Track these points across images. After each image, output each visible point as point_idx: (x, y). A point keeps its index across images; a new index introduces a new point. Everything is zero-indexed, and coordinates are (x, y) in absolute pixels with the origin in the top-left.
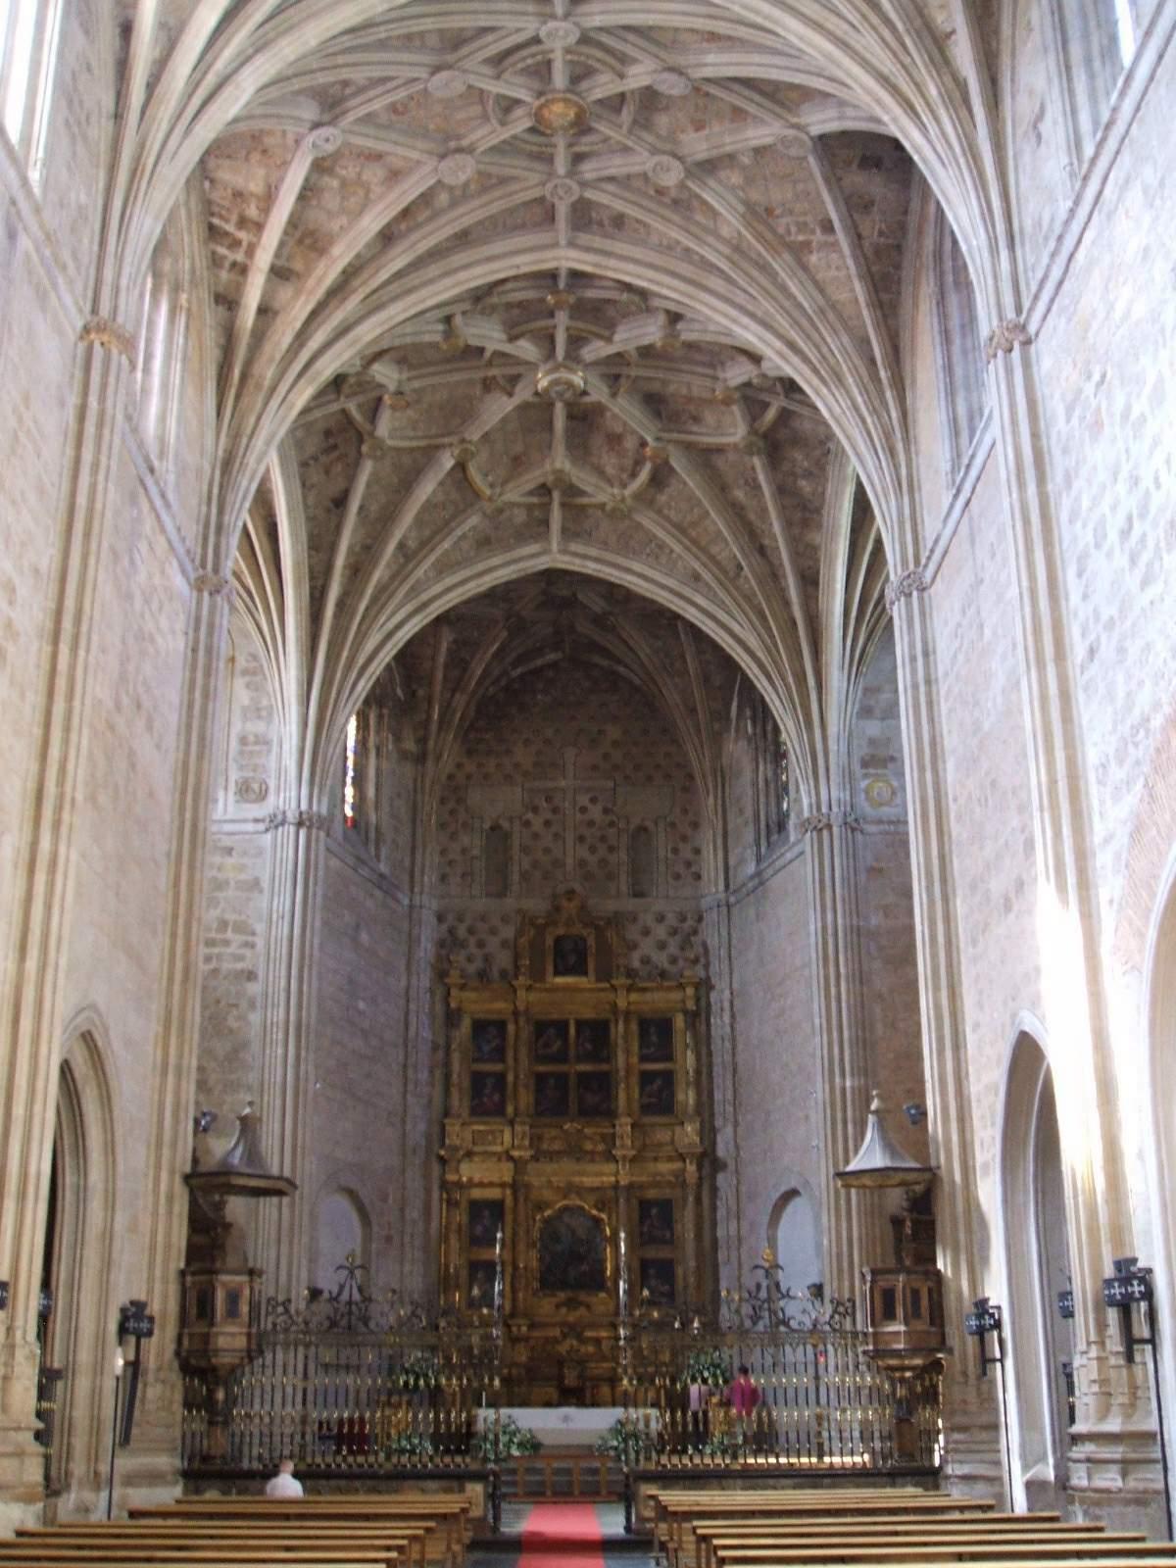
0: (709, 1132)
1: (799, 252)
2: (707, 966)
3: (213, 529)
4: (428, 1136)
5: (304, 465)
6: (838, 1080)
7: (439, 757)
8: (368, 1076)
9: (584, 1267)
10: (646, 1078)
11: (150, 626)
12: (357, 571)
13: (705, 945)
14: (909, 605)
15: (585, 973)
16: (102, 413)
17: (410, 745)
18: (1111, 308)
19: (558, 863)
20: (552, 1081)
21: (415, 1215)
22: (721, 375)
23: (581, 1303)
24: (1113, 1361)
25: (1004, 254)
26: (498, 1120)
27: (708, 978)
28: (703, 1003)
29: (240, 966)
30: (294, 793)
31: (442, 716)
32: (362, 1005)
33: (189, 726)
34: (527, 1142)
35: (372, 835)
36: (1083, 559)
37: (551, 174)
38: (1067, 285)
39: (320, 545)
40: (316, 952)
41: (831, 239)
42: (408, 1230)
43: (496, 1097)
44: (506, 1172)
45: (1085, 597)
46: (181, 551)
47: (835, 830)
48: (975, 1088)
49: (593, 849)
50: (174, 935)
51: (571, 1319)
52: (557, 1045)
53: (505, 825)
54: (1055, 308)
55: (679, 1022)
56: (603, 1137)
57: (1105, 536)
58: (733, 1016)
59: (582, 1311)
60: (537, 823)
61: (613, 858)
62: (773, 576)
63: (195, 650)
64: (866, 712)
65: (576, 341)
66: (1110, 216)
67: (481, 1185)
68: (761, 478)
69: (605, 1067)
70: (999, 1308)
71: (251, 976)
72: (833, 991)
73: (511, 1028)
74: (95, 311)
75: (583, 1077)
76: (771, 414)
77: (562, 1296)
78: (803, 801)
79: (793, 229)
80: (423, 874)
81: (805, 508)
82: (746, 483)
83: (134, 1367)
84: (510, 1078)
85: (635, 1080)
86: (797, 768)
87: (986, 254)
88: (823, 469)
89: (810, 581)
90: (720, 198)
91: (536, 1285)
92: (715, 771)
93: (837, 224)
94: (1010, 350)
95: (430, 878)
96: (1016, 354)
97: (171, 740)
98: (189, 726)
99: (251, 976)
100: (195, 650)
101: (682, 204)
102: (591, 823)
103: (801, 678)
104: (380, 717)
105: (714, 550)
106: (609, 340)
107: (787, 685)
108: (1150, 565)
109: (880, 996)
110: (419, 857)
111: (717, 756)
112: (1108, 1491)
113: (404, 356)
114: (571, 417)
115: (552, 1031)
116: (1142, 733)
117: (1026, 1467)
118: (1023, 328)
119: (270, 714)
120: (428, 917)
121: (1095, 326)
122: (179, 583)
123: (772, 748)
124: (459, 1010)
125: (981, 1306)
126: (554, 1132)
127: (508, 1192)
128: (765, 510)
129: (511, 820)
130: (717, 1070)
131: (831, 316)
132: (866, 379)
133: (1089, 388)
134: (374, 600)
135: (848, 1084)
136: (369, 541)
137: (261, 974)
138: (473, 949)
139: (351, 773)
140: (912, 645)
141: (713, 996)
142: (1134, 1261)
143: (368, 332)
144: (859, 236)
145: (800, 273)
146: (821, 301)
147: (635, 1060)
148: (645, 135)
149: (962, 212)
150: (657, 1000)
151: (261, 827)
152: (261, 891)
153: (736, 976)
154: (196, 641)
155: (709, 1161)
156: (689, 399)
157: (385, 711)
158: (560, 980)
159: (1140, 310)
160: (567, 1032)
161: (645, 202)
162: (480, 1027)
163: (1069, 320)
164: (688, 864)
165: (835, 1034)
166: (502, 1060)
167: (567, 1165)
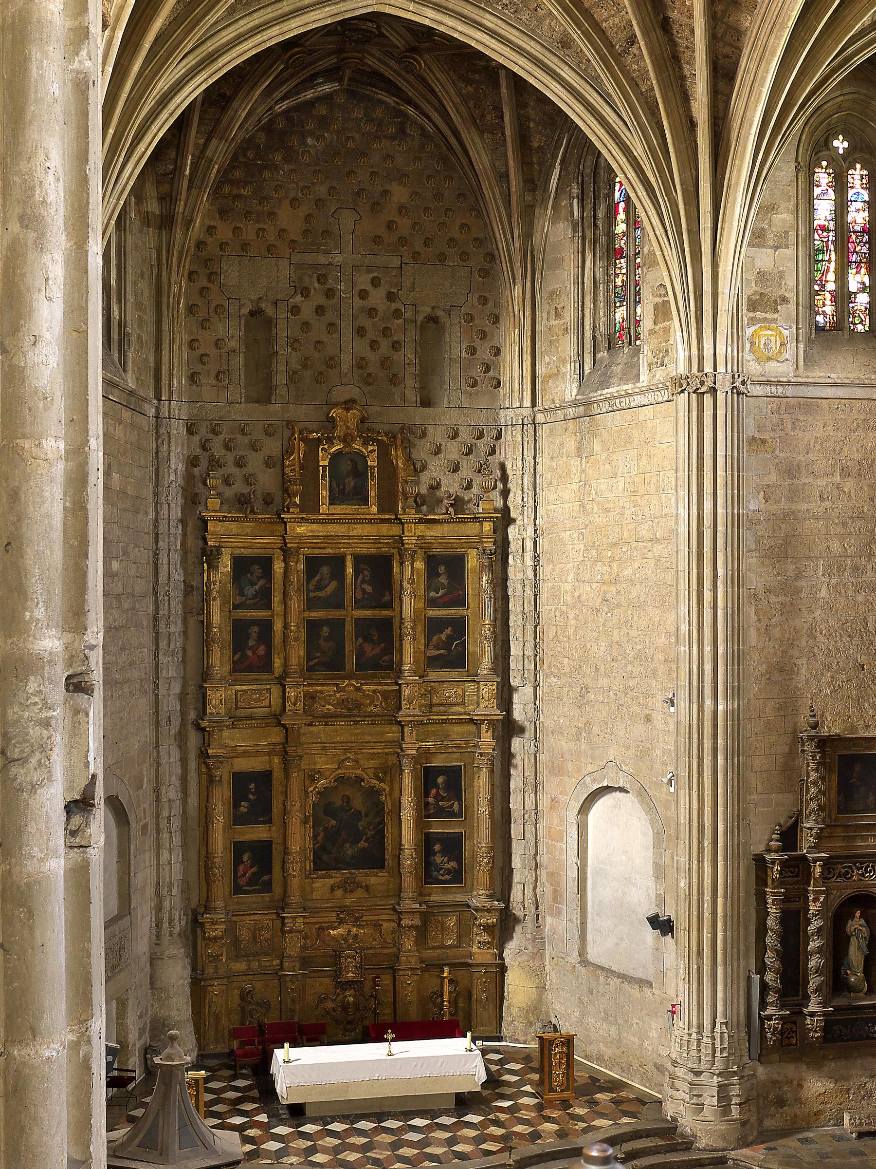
7: (189, 222)
9: (362, 844)
10: (434, 626)
13: (503, 467)
19: (332, 362)
21: (172, 795)
23: (359, 885)
42: (165, 813)
43: (261, 651)
47: (721, 396)
49: (374, 345)
51: (348, 902)
53: (270, 311)
55: (472, 561)
56: (386, 695)
58: (536, 558)
59: (360, 893)
60: (307, 311)
61: (397, 357)
67: (245, 754)
69: (386, 613)
72: (708, 594)
73: (278, 567)
77: (337, 877)
80: (171, 376)
84: (278, 626)
91: (309, 866)
95: (179, 381)
107: (674, 204)
110: (165, 352)
111: (528, 236)
115: (325, 570)
120: (178, 429)
123: (603, 240)
124: (218, 549)
127: (276, 760)
135: (720, 708)
138: (231, 469)
147: (421, 605)
166: (269, 606)
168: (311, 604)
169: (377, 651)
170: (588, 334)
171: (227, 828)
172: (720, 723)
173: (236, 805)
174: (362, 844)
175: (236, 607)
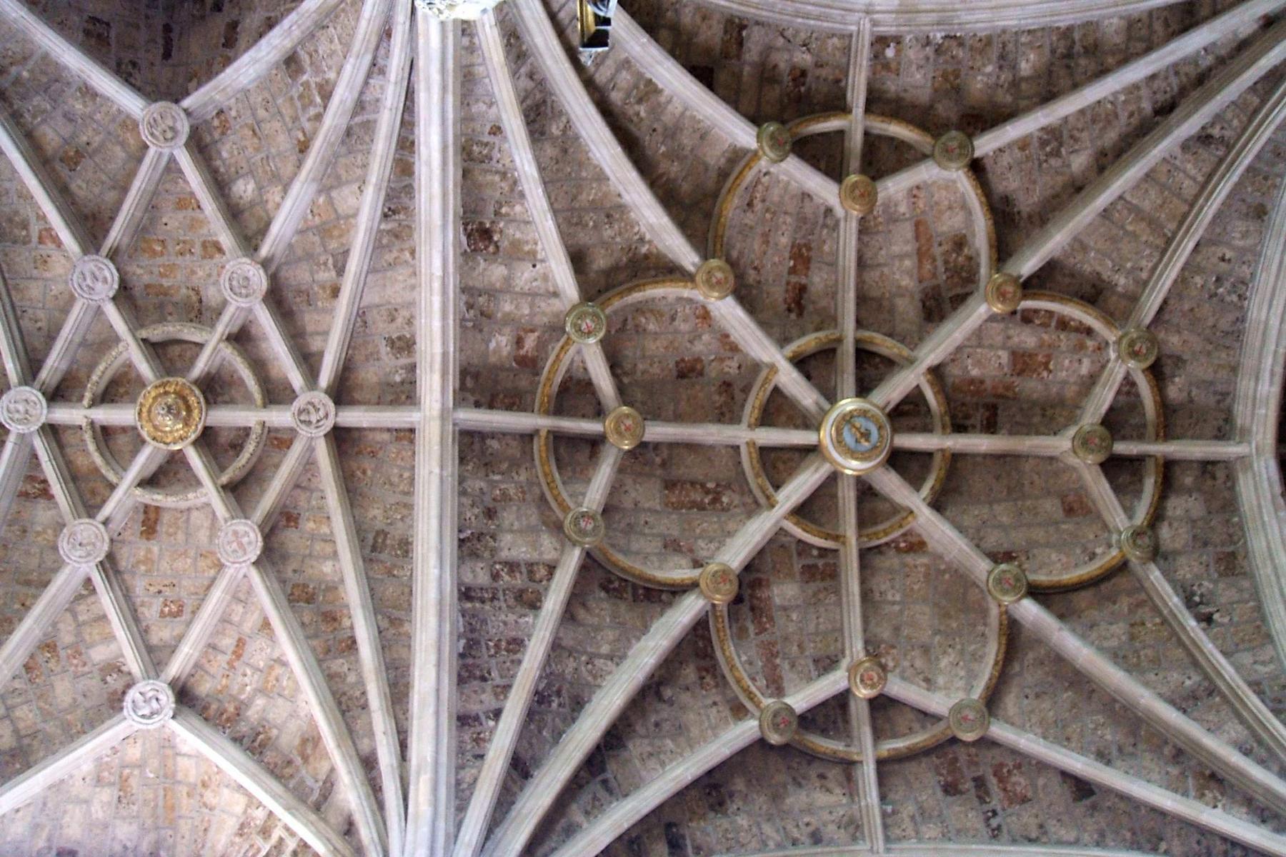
5: (995, 834)
81: (1069, 55)
82: (1056, 153)
88: (988, 41)
156: (921, 254)
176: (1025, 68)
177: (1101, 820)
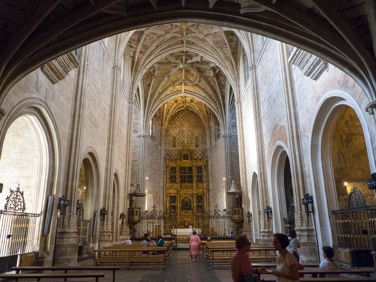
0: (208, 185)
1: (221, 48)
2: (207, 158)
3: (131, 93)
4: (163, 185)
6: (228, 177)
7: (165, 125)
8: (154, 176)
9: (188, 206)
10: (198, 176)
11: (122, 110)
12: (152, 96)
14: (238, 105)
15: (188, 160)
16: (116, 80)
17: (160, 123)
18: (267, 66)
19: (184, 142)
20: (183, 177)
22: (209, 65)
24: (266, 221)
25: (252, 54)
26: (175, 183)
27: (208, 160)
28: (207, 164)
29: (134, 159)
30: (142, 132)
31: (165, 118)
32: (153, 165)
33: (128, 125)
34: (179, 187)
35: (154, 138)
36: (263, 102)
37: (183, 36)
38: (261, 60)
39: (146, 92)
40: (146, 157)
41: (226, 46)
42: (161, 201)
43: (174, 179)
44: (176, 191)
45: (263, 108)
46: (127, 98)
48: (248, 180)
49: (189, 139)
50: (127, 157)
52: (184, 171)
53: (175, 136)
54: (259, 63)
55: (203, 167)
57: (266, 100)
58: (212, 166)
60: (180, 136)
61: (192, 141)
62: (217, 97)
63: (129, 113)
64: (232, 118)
65: (186, 60)
66: (267, 51)
68: (216, 81)
69: (191, 174)
70: (251, 213)
71: (136, 161)
72: (227, 163)
73: (177, 168)
74: (115, 64)
75: (188, 176)
76: (217, 71)
78: (222, 132)
79: (221, 45)
81: (223, 86)
83: (122, 223)
84: (176, 176)
85: (196, 176)
86: (221, 128)
87: (249, 54)
89: (223, 97)
90: (209, 40)
92: (209, 127)
93: (227, 44)
94: (253, 69)
95: (163, 145)
96: (254, 70)
97: (126, 127)
98: (128, 125)
99: (136, 161)
100: (129, 113)
101: (203, 40)
102: (189, 135)
103: (222, 113)
104: (155, 119)
105: (208, 92)
106: (192, 60)
108: (271, 105)
109: (235, 163)
111: (209, 125)
112: (265, 240)
113: (159, 63)
114: (185, 71)
115: (183, 169)
116: (270, 130)
117: (255, 237)
118: (255, 66)
119: (138, 119)
120: (163, 151)
121: (265, 68)
122: (126, 103)
125: (249, 213)
126: (184, 185)
127: (176, 194)
128: (216, 86)
129: (176, 135)
130: (209, 175)
131: (227, 59)
132: (232, 69)
133: (264, 77)
134: (155, 101)
136: (154, 91)
137: (138, 161)
139: (151, 128)
140: (239, 111)
141: (209, 163)
142: (269, 206)
143: (154, 61)
144: (231, 46)
145: (222, 52)
146: (225, 56)
147: (196, 173)
148: (197, 30)
149: (246, 47)
150: (200, 164)
151: (137, 137)
152: (137, 147)
153: (212, 160)
154: (129, 111)
155: (209, 190)
157: (156, 118)
158: (184, 161)
159: (271, 67)
160: (185, 169)
161: (197, 40)
162: (172, 168)
163: (261, 66)
164: (204, 142)
165: (227, 170)
166: (175, 174)
167: (186, 190)
168: (181, 173)
169: (190, 180)
170: (216, 136)
171: (169, 204)
172: (230, 179)
173: (171, 201)
174: (188, 206)
175: (171, 174)
176: (222, 82)
177: (146, 87)
